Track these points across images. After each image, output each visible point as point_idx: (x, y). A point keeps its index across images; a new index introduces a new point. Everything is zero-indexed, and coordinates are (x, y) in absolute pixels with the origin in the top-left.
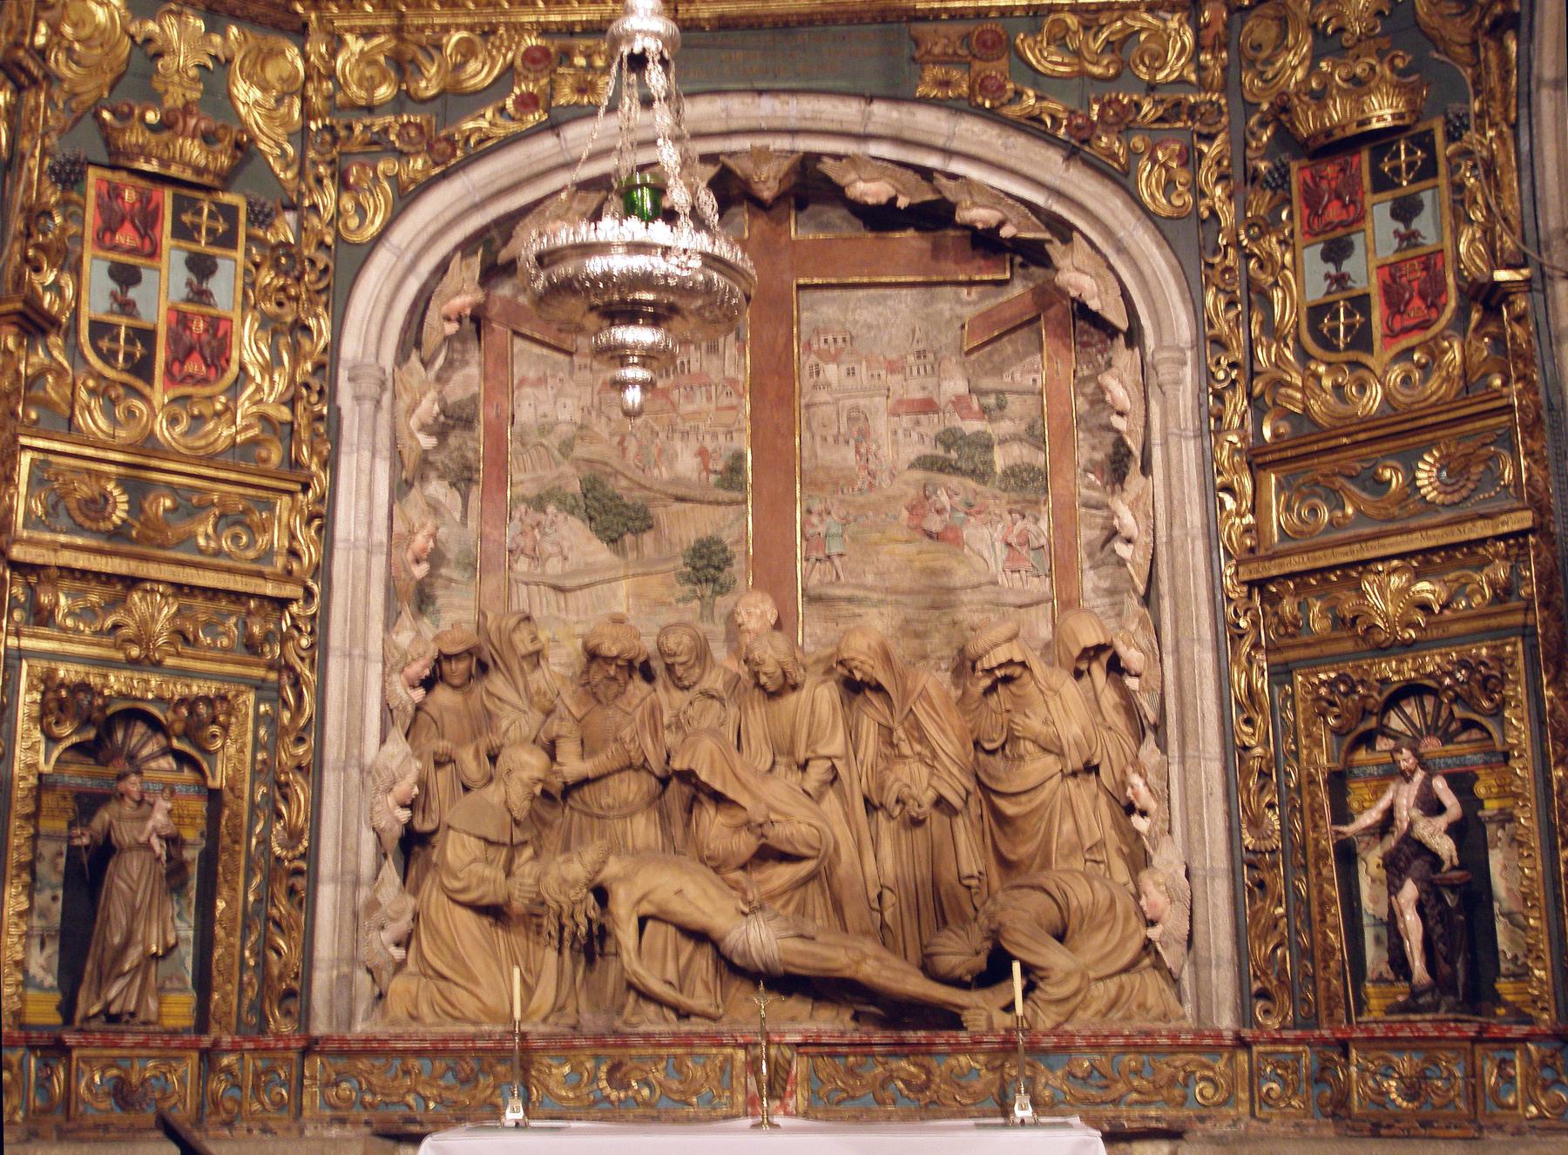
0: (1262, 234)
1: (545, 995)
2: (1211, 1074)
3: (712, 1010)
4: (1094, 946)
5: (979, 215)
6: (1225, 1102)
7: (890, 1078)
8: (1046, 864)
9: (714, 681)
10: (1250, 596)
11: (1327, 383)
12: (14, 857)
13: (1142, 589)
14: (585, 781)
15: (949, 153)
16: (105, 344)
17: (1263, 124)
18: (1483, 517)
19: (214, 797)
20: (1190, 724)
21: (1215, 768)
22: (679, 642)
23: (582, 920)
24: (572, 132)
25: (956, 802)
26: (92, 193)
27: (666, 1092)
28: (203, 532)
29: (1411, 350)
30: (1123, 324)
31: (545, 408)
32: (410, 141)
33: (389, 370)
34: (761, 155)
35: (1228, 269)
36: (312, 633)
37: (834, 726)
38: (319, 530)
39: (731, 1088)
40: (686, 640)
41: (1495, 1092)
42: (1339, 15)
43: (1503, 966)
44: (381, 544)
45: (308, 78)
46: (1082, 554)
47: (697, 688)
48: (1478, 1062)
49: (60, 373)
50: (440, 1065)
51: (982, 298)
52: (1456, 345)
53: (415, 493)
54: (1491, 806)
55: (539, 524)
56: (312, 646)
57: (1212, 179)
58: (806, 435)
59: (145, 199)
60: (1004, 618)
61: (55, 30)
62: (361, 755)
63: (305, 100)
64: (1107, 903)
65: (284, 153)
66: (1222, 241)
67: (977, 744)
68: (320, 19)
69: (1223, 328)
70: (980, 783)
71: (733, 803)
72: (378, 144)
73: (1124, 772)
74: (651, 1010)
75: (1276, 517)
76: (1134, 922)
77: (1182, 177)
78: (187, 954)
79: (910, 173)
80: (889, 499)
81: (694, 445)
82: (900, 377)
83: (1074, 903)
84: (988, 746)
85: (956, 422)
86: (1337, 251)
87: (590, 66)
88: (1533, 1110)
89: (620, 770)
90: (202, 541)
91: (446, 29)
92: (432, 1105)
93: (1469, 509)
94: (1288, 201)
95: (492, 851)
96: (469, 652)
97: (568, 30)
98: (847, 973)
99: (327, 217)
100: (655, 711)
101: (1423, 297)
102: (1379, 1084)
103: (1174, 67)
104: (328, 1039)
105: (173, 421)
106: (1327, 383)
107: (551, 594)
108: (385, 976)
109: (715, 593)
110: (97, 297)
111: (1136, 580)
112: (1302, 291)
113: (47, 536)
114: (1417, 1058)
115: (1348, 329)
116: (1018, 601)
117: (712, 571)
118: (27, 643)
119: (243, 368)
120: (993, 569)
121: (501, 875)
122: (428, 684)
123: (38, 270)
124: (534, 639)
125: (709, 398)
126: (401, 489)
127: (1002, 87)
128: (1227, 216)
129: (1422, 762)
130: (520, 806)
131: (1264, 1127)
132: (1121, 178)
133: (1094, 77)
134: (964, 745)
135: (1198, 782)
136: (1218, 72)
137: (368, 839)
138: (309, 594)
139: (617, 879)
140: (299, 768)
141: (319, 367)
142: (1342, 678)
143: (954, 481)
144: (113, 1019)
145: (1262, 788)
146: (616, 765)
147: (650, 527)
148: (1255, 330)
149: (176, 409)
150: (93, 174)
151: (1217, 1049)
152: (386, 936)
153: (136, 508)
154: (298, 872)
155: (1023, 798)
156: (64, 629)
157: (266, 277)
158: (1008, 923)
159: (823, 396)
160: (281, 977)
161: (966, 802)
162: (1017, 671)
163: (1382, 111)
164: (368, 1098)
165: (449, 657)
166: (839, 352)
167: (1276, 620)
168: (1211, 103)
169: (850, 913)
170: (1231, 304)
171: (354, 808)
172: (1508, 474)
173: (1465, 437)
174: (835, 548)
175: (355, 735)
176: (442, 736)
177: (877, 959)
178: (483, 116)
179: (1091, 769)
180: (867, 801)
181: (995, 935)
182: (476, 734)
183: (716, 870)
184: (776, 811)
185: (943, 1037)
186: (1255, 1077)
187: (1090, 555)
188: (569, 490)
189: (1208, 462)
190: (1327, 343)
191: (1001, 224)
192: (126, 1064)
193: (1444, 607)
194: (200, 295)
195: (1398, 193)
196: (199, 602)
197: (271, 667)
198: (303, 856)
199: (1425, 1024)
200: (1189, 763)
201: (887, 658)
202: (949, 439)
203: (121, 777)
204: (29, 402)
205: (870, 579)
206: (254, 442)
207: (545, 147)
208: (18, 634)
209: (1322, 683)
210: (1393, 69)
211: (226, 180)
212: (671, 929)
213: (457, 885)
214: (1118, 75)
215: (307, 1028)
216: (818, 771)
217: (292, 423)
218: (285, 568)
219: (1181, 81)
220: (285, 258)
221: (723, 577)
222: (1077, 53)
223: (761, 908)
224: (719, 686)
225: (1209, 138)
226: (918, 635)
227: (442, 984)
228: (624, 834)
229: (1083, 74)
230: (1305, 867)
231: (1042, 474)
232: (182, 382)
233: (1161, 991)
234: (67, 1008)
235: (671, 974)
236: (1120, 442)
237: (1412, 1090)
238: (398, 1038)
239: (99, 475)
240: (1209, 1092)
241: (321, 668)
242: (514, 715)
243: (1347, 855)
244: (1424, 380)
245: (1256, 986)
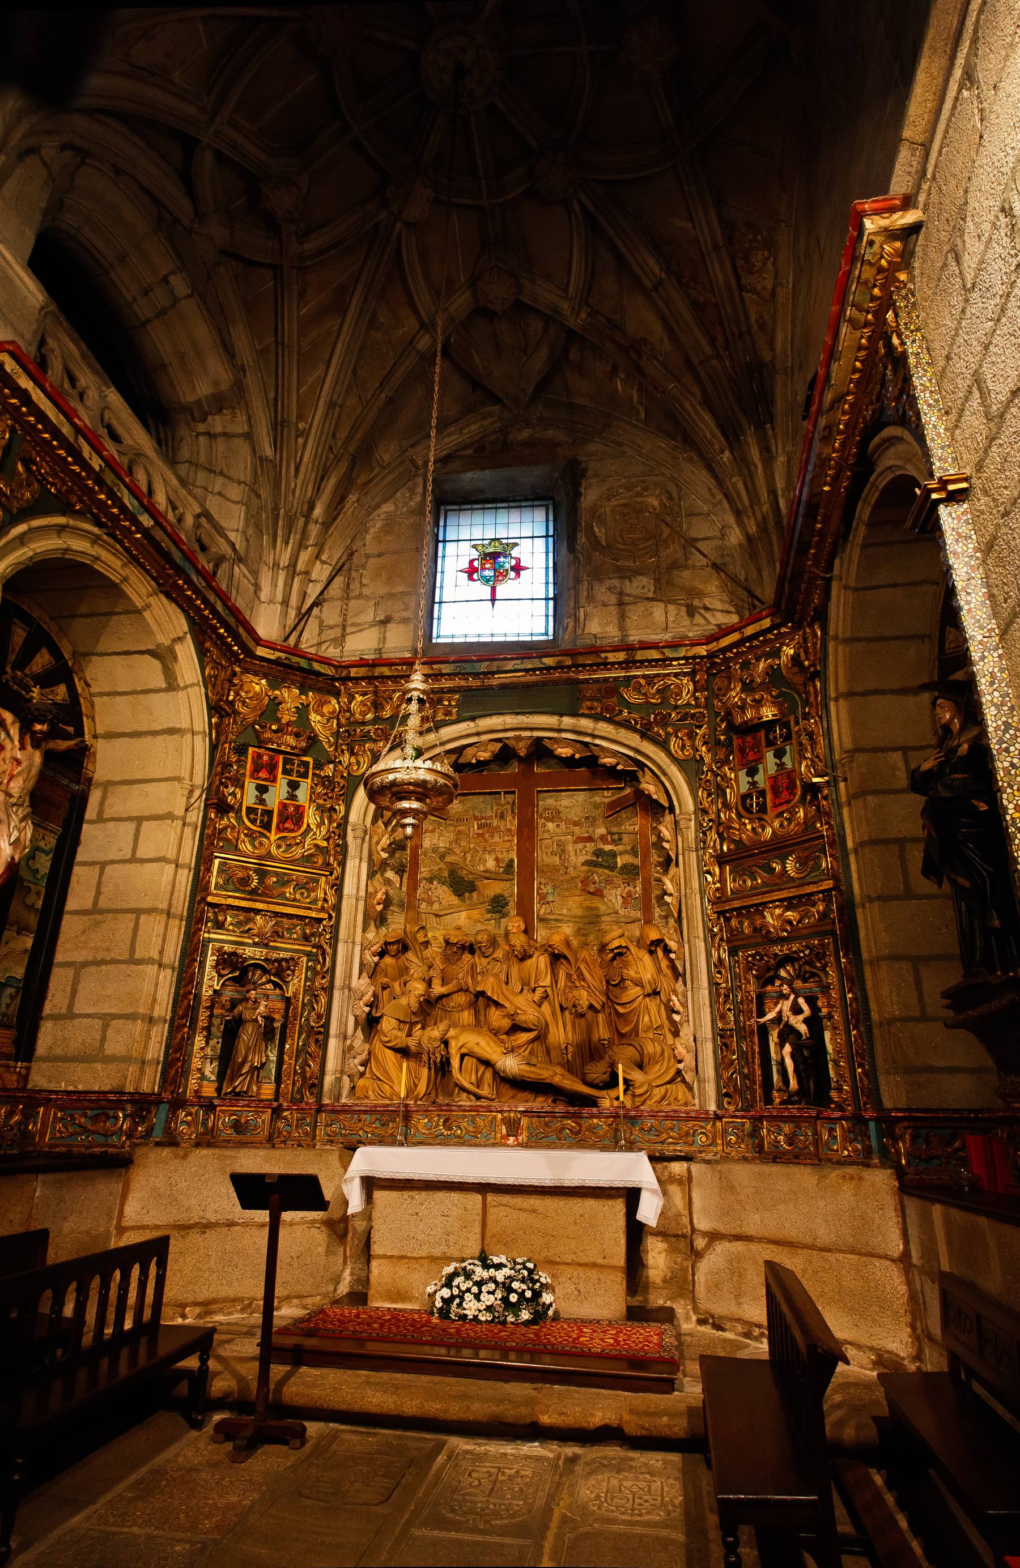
0: (722, 766)
1: (422, 1088)
4: (655, 1071)
5: (608, 761)
6: (710, 1145)
7: (563, 1129)
8: (637, 1034)
9: (499, 954)
10: (719, 918)
11: (749, 827)
12: (200, 1024)
13: (676, 915)
14: (442, 996)
16: (252, 816)
17: (722, 721)
18: (811, 883)
19: (288, 1001)
20: (695, 973)
21: (706, 992)
22: (483, 938)
23: (438, 1055)
25: (598, 1007)
26: (250, 757)
27: (468, 1131)
28: (289, 891)
29: (783, 813)
30: (666, 805)
31: (435, 841)
34: (519, 738)
35: (708, 781)
38: (336, 891)
39: (495, 1131)
40: (485, 937)
41: (827, 1143)
42: (751, 675)
43: (833, 1084)
45: (340, 712)
46: (654, 901)
48: (819, 1128)
49: (233, 827)
51: (613, 795)
52: (801, 810)
53: (378, 875)
54: (825, 1011)
58: (540, 852)
59: (271, 758)
60: (621, 927)
61: (237, 694)
62: (350, 983)
63: (338, 720)
65: (329, 741)
66: (705, 769)
67: (608, 982)
71: (503, 1006)
72: (366, 737)
74: (465, 1095)
75: (729, 885)
76: (673, 1060)
78: (273, 1067)
79: (578, 745)
80: (573, 878)
81: (493, 856)
83: (646, 1052)
85: (601, 846)
86: (752, 772)
87: (450, 704)
88: (846, 1152)
89: (458, 992)
90: (288, 895)
91: (394, 691)
93: (808, 879)
94: (732, 752)
96: (398, 942)
97: (442, 691)
98: (548, 1081)
100: (473, 967)
101: (788, 790)
102: (776, 1137)
103: (685, 698)
104: (327, 1105)
105: (279, 847)
106: (749, 827)
110: (249, 796)
112: (738, 789)
113: (224, 893)
114: (792, 1125)
115: (757, 804)
116: (626, 920)
118: (212, 936)
119: (308, 825)
122: (382, 954)
123: (227, 787)
124: (426, 936)
126: (371, 875)
127: (614, 709)
128: (707, 759)
129: (793, 990)
130: (415, 1006)
132: (663, 745)
133: (652, 703)
137: (351, 1020)
138: (330, 917)
139: (454, 1038)
140: (323, 988)
141: (339, 825)
142: (757, 954)
143: (600, 870)
144: (238, 1094)
145: (725, 1002)
148: (720, 806)
149: (280, 842)
150: (251, 750)
151: (707, 1119)
152: (356, 1061)
153: (261, 881)
154: (320, 1033)
156: (228, 930)
157: (319, 789)
159: (546, 836)
161: (603, 1007)
162: (625, 950)
163: (768, 713)
165: (390, 943)
166: (553, 817)
169: (553, 1054)
170: (709, 795)
171: (345, 1006)
172: (824, 865)
173: (806, 849)
174: (550, 898)
176: (386, 976)
177: (562, 1075)
179: (656, 993)
180: (561, 1006)
182: (401, 975)
183: (495, 1034)
185: (585, 1111)
187: (658, 902)
190: (749, 810)
191: (617, 764)
192: (240, 1113)
193: (799, 922)
194: (292, 797)
195: (776, 747)
196: (285, 920)
197: (313, 947)
198: (322, 1026)
199: (794, 1110)
201: (568, 944)
202: (598, 853)
203: (248, 991)
204: (219, 839)
205: (564, 912)
206: (311, 855)
208: (209, 932)
209: (750, 955)
210: (772, 696)
211: (305, 752)
213: (386, 1039)
214: (661, 703)
215: (321, 1100)
219: (688, 704)
220: (328, 782)
222: (645, 694)
223: (512, 1051)
224: (500, 956)
225: (700, 727)
226: (584, 935)
229: (648, 702)
230: (745, 1038)
231: (637, 867)
232: (283, 831)
233: (685, 1093)
234: (219, 1090)
235: (473, 1079)
236: (669, 856)
237: (791, 1140)
238: (356, 1105)
239: (247, 868)
240: (704, 1139)
243: (763, 1032)
244: (789, 825)
245: (724, 1091)
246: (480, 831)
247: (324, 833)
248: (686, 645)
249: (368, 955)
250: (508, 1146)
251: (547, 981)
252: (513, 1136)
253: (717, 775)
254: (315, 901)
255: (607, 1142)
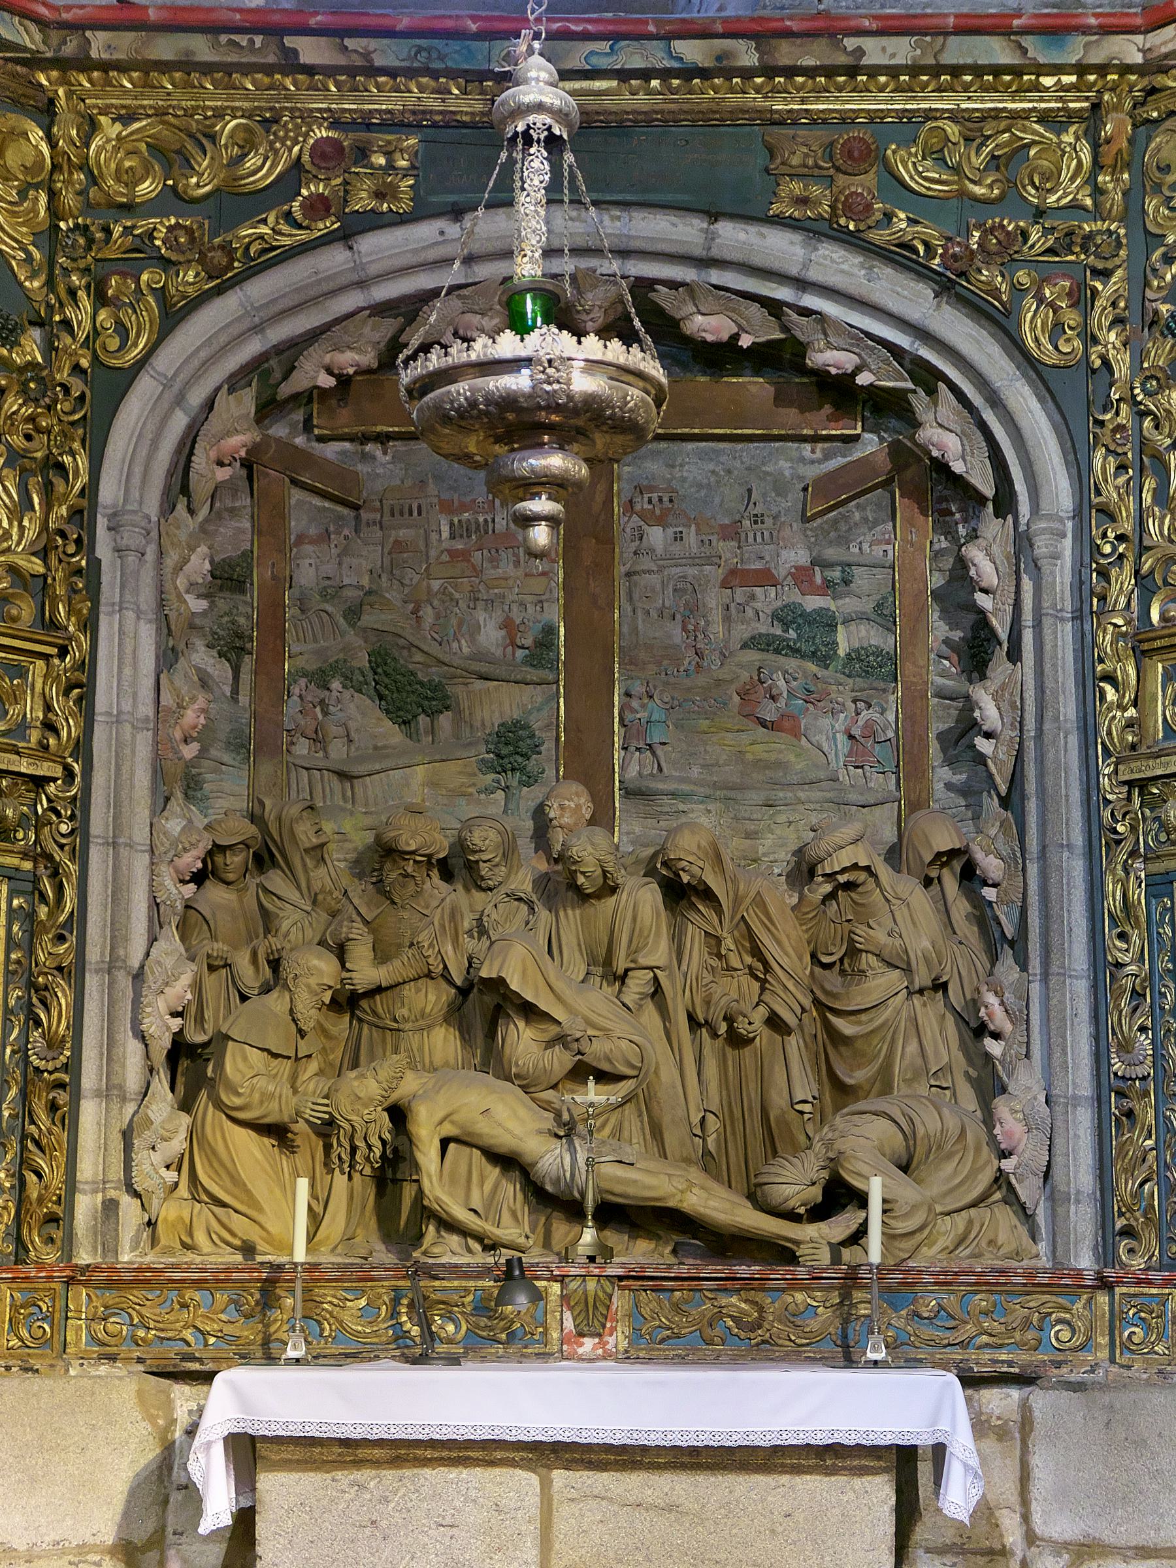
2: (1068, 1316)
3: (522, 1240)
7: (720, 1315)
13: (1003, 789)
15: (802, 284)
20: (1055, 939)
23: (375, 1141)
24: (369, 244)
31: (329, 569)
32: (179, 248)
33: (154, 519)
36: (72, 818)
37: (658, 934)
38: (79, 700)
44: (147, 719)
47: (503, 890)
50: (221, 1297)
55: (322, 702)
56: (73, 831)
57: (1106, 323)
63: (52, 195)
64: (958, 1132)
65: (29, 258)
67: (813, 956)
68: (69, 95)
69: (1110, 494)
70: (816, 1002)
73: (978, 990)
74: (454, 1240)
77: (1071, 318)
79: (754, 309)
80: (719, 682)
81: (498, 615)
82: (734, 544)
83: (921, 1131)
84: (825, 960)
87: (391, 167)
91: (219, 114)
92: (212, 1340)
95: (275, 1062)
97: (365, 123)
98: (671, 1204)
99: (81, 336)
107: (336, 781)
108: (155, 1202)
109: (522, 784)
111: (998, 779)
116: (862, 800)
117: (520, 759)
120: (833, 764)
121: (287, 1090)
122: (199, 878)
125: (517, 563)
126: (168, 658)
131: (1126, 1373)
133: (976, 199)
134: (800, 959)
135: (1062, 1002)
136: (1119, 197)
138: (69, 774)
140: (60, 969)
141: (76, 513)
143: (792, 664)
146: (412, 973)
147: (447, 708)
151: (1076, 1289)
152: (157, 1158)
154: (61, 1085)
155: (863, 1017)
158: (849, 1152)
159: (646, 563)
160: (41, 1200)
162: (862, 876)
164: (141, 1333)
166: (665, 513)
167: (1156, 825)
168: (1110, 232)
175: (117, 935)
176: (214, 937)
178: (264, 221)
179: (940, 986)
180: (691, 1018)
181: (833, 1164)
183: (525, 1089)
184: (594, 1026)
186: (1115, 1320)
188: (356, 664)
189: (1086, 649)
191: (858, 370)
197: (25, 856)
198: (65, 1068)
200: (1053, 981)
207: (335, 259)
212: (477, 1153)
213: (237, 1101)
216: (638, 983)
217: (45, 577)
218: (40, 743)
219: (1075, 206)
221: (532, 764)
225: (1105, 274)
227: (219, 1211)
228: (421, 1050)
229: (963, 194)
238: (175, 1267)
241: (81, 856)
242: (299, 915)
246: (459, 545)
247: (31, 534)
248: (1085, 30)
249: (168, 881)
250: (581, 1359)
251: (659, 953)
252: (592, 1335)
253: (1143, 414)
254: (21, 729)
255: (828, 1347)
